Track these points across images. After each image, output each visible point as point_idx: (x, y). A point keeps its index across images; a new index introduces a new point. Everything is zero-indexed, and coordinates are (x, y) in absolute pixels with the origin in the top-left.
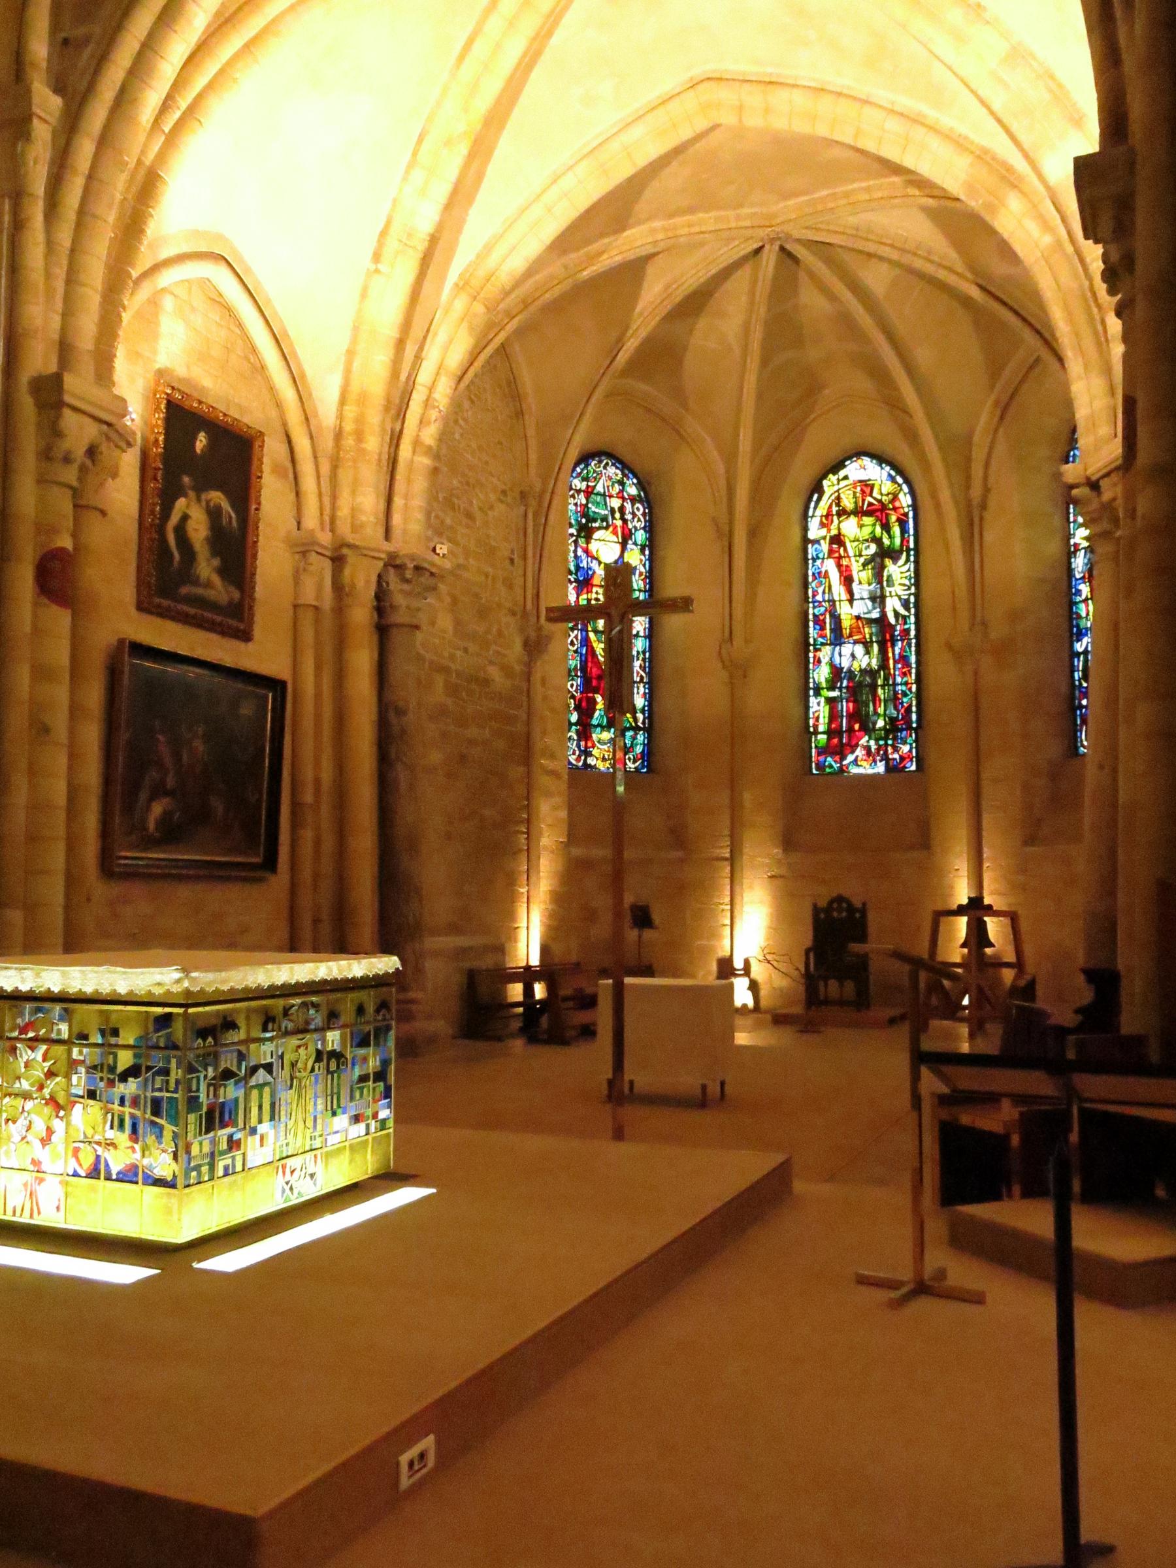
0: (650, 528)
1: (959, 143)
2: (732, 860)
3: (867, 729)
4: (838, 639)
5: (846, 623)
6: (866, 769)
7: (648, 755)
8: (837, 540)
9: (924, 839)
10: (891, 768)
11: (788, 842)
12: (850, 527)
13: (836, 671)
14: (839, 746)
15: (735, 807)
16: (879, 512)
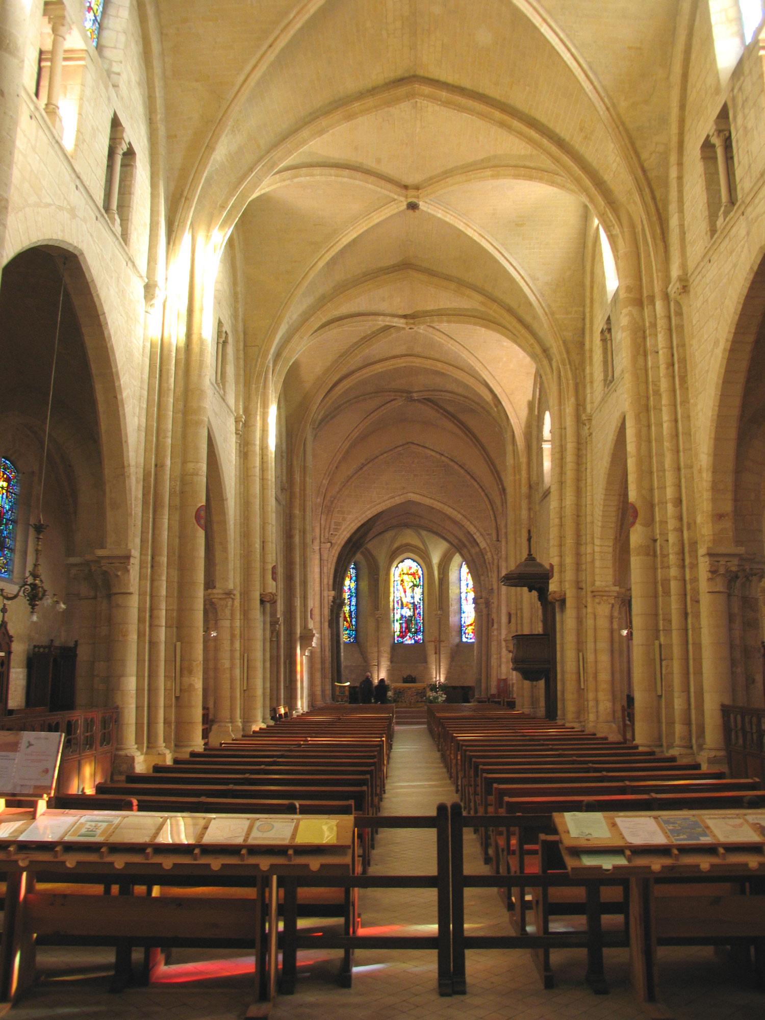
0: (356, 576)
1: (457, 537)
2: (378, 665)
3: (410, 631)
4: (402, 607)
5: (405, 603)
6: (409, 642)
7: (355, 638)
8: (402, 581)
9: (425, 660)
10: (416, 641)
11: (391, 662)
12: (406, 577)
13: (402, 616)
14: (403, 635)
15: (379, 651)
16: (413, 574)
